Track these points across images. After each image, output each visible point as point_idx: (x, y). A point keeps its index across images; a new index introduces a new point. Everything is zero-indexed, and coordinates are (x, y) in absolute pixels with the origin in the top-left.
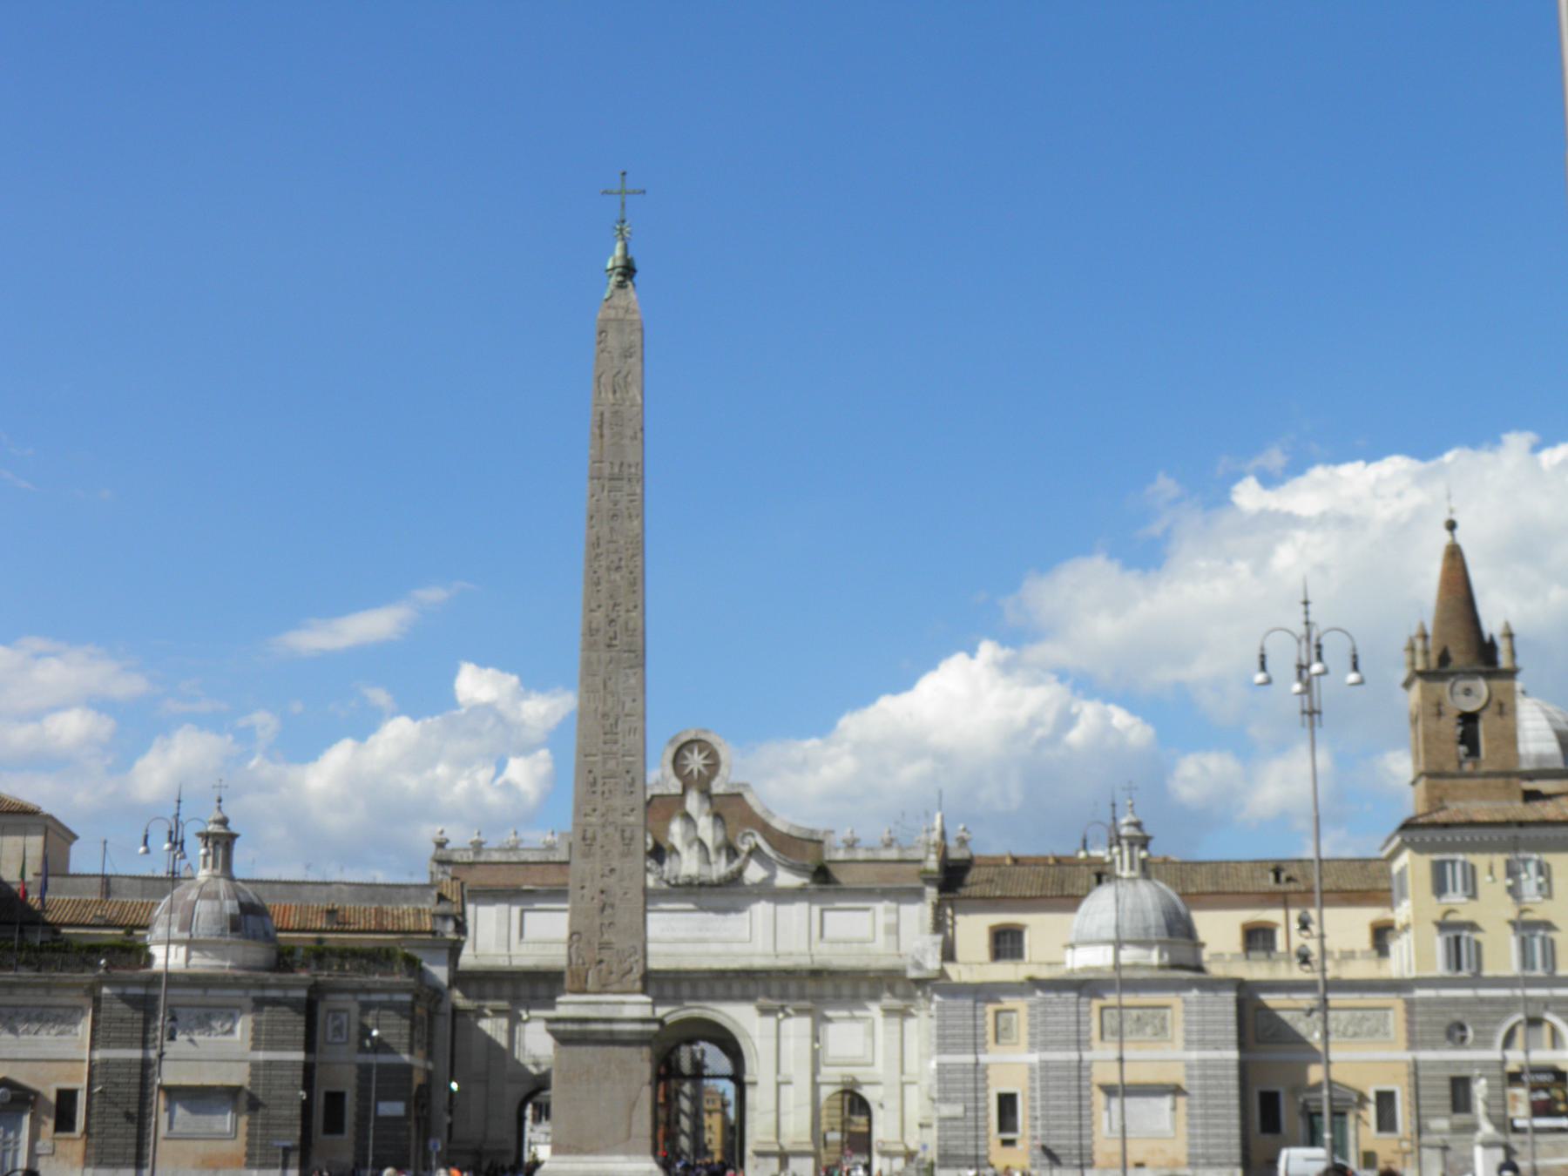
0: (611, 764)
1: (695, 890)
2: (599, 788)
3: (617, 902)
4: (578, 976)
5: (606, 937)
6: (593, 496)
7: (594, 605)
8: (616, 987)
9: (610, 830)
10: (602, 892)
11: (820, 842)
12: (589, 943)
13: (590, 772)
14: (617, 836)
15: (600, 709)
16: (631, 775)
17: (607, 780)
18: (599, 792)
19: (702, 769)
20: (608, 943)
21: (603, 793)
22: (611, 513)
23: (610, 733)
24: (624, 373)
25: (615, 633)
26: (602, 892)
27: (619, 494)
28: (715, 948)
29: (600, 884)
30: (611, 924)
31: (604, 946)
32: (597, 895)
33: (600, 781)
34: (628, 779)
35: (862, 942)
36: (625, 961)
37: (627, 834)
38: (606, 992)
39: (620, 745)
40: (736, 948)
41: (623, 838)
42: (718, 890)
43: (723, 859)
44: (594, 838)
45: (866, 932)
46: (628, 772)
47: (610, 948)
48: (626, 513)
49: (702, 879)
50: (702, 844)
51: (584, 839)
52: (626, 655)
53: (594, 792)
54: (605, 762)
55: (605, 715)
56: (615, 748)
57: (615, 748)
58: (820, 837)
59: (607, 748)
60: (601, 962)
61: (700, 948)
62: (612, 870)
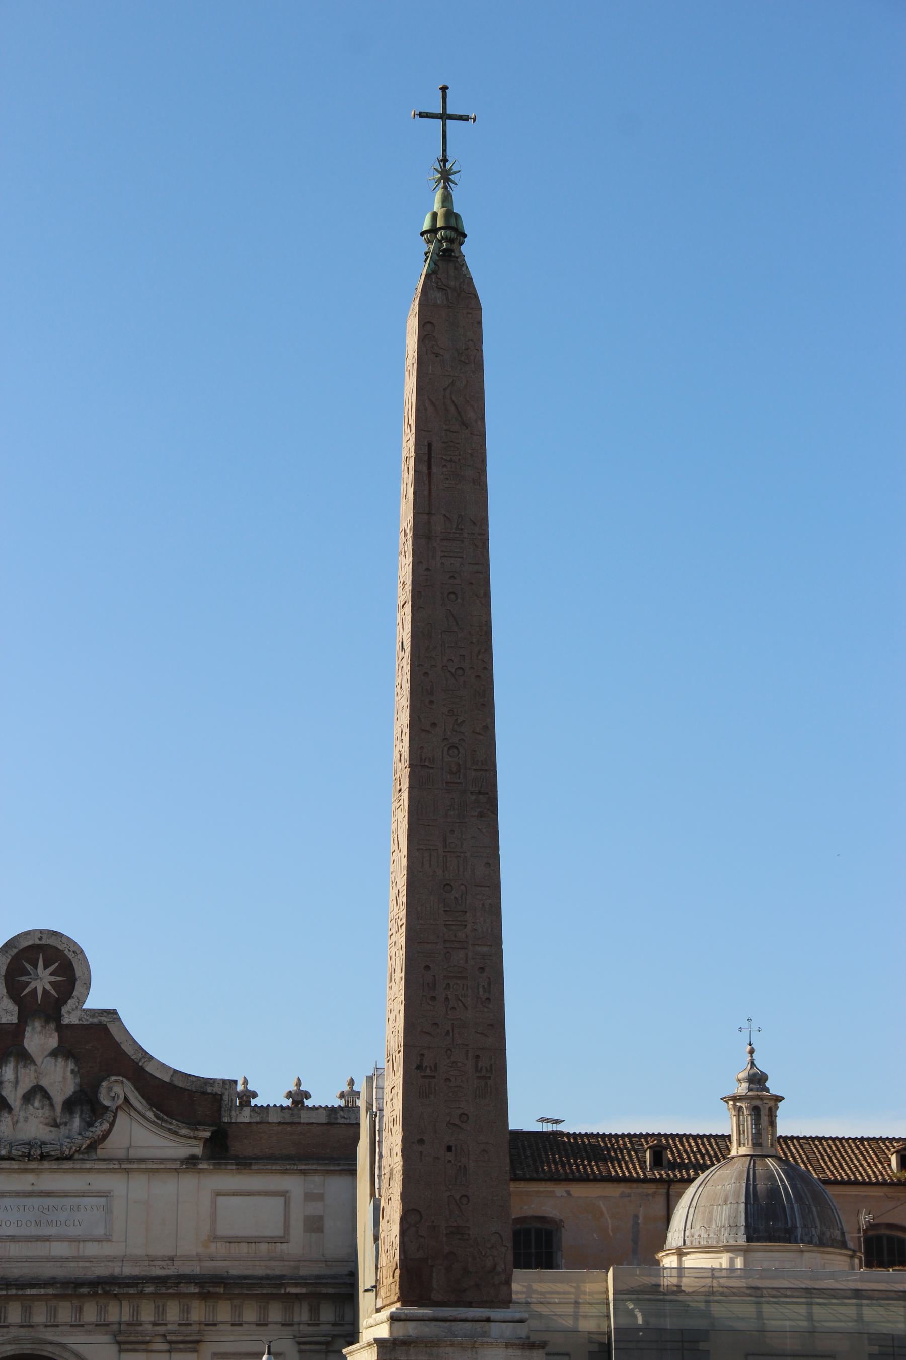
1: (33, 1165)
10: (449, 1149)
11: (217, 1099)
19: (48, 987)
21: (447, 999)
26: (449, 1149)
28: (59, 1249)
35: (272, 1241)
38: (458, 1304)
40: (91, 1249)
41: (477, 1069)
42: (67, 1165)
43: (77, 1122)
44: (435, 1068)
45: (278, 1232)
49: (45, 1150)
50: (46, 1095)
51: (419, 1067)
52: (473, 798)
53: (434, 998)
58: (217, 1089)
61: (40, 1250)
62: (464, 1116)
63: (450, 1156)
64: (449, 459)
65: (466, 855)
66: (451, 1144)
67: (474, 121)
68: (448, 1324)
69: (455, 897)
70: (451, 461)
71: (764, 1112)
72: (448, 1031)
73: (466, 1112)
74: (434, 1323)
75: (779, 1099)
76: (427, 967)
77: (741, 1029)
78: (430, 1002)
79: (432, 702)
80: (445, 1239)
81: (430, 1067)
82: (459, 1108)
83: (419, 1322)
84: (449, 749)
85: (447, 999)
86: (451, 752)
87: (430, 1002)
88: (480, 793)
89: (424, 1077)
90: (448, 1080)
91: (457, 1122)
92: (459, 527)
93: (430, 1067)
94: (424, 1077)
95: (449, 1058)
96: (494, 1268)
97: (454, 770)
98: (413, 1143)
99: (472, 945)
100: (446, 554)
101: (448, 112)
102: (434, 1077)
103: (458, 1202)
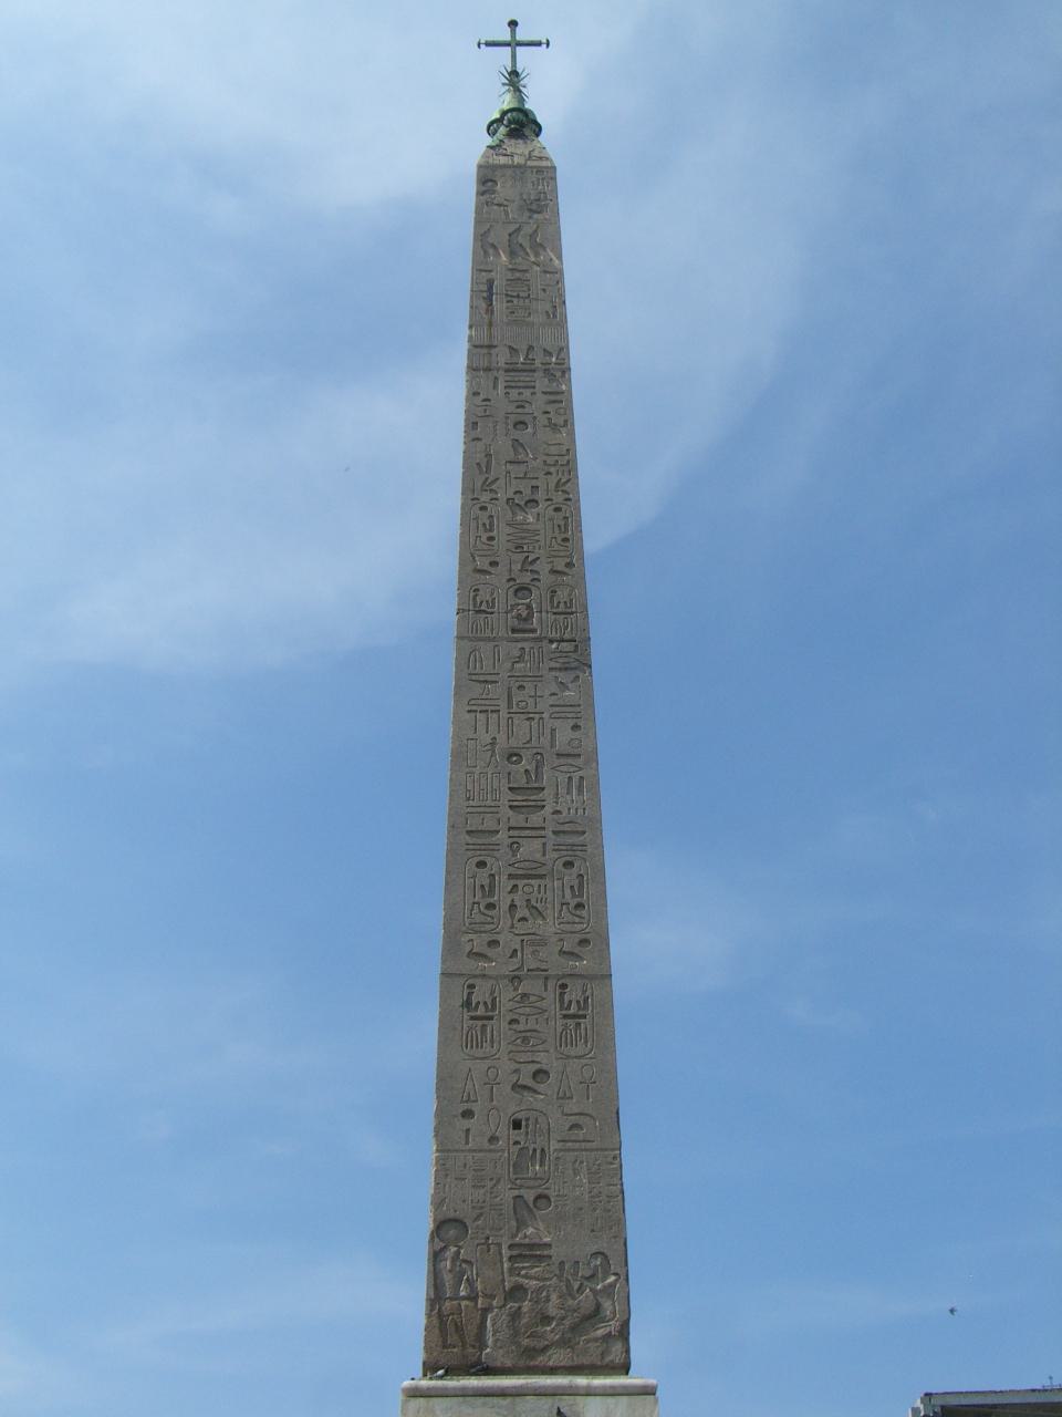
0: (530, 849)
2: (503, 899)
4: (459, 1329)
6: (476, 394)
7: (481, 563)
8: (557, 1357)
10: (517, 1125)
13: (481, 864)
14: (551, 995)
15: (501, 738)
16: (575, 870)
17: (521, 883)
18: (504, 906)
20: (531, 1246)
21: (513, 906)
22: (513, 418)
23: (527, 795)
24: (528, 230)
25: (529, 607)
27: (527, 393)
29: (512, 1106)
30: (542, 1198)
31: (530, 1253)
32: (504, 1130)
33: (504, 884)
34: (570, 877)
36: (580, 1289)
37: (573, 994)
39: (549, 809)
46: (568, 864)
47: (540, 1258)
48: (543, 420)
51: (467, 1004)
53: (491, 906)
54: (514, 846)
55: (513, 756)
56: (535, 819)
57: (535, 819)
60: (517, 1292)
62: (540, 1074)
64: (515, 294)
65: (544, 716)
66: (518, 1116)
67: (548, 45)
68: (509, 1399)
69: (526, 771)
70: (518, 296)
72: (516, 951)
73: (545, 1067)
74: (482, 1399)
78: (486, 912)
79: (491, 539)
81: (485, 1003)
82: (533, 1062)
84: (516, 591)
86: (520, 594)
87: (486, 912)
89: (472, 1018)
90: (512, 1022)
91: (529, 1082)
92: (530, 357)
93: (485, 1003)
94: (472, 1018)
95: (516, 989)
97: (524, 614)
98: (455, 1116)
99: (554, 832)
100: (513, 384)
101: (518, 38)
102: (491, 1018)
103: (531, 1205)
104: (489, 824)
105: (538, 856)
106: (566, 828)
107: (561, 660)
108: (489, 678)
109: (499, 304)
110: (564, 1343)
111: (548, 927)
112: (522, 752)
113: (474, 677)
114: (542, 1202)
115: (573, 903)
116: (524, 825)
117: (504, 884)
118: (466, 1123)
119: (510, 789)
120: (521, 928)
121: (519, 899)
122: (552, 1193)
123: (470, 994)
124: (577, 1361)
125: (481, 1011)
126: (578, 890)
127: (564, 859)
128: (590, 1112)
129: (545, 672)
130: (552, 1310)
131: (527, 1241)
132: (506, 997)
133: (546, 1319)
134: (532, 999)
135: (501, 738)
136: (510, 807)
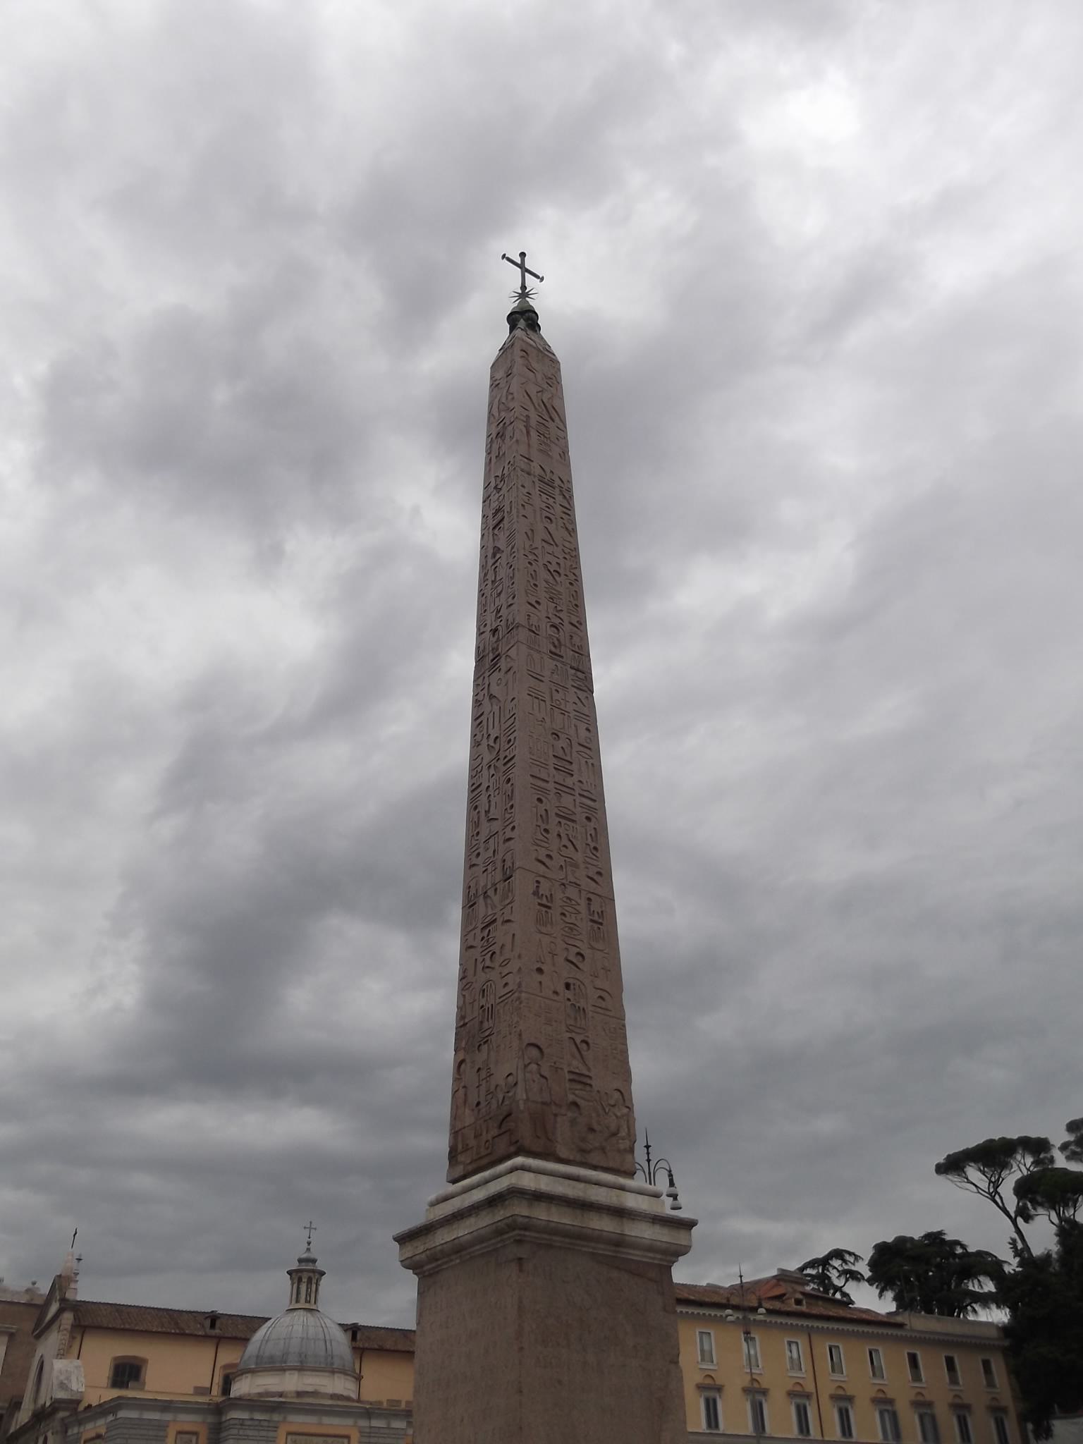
0: (567, 800)
3: (589, 1009)
5: (577, 1065)
8: (596, 1158)
9: (571, 892)
12: (557, 1069)
14: (583, 903)
15: (548, 720)
17: (563, 821)
26: (568, 986)
32: (561, 988)
33: (554, 820)
37: (595, 907)
39: (576, 778)
51: (536, 893)
52: (573, 671)
55: (556, 735)
56: (569, 781)
59: (559, 777)
63: (568, 994)
66: (571, 981)
71: (314, 1281)
73: (582, 952)
75: (322, 1274)
76: (540, 800)
77: (305, 1228)
78: (543, 833)
80: (568, 1085)
83: (552, 1177)
85: (559, 835)
87: (543, 833)
88: (578, 670)
89: (539, 904)
90: (563, 914)
91: (572, 958)
94: (539, 904)
96: (618, 1130)
104: (544, 776)
105: (571, 807)
106: (585, 793)
107: (578, 683)
108: (538, 677)
109: (533, 434)
110: (603, 1149)
111: (579, 857)
112: (559, 734)
113: (530, 673)
114: (584, 1045)
115: (593, 845)
116: (562, 783)
117: (554, 820)
118: (539, 977)
119: (554, 756)
120: (564, 852)
121: (562, 831)
122: (590, 1041)
123: (538, 887)
124: (611, 1165)
125: (544, 901)
126: (595, 838)
127: (587, 815)
128: (608, 990)
129: (569, 686)
130: (596, 1127)
131: (577, 1071)
132: (559, 895)
133: (592, 1130)
134: (573, 902)
135: (548, 720)
136: (555, 768)
